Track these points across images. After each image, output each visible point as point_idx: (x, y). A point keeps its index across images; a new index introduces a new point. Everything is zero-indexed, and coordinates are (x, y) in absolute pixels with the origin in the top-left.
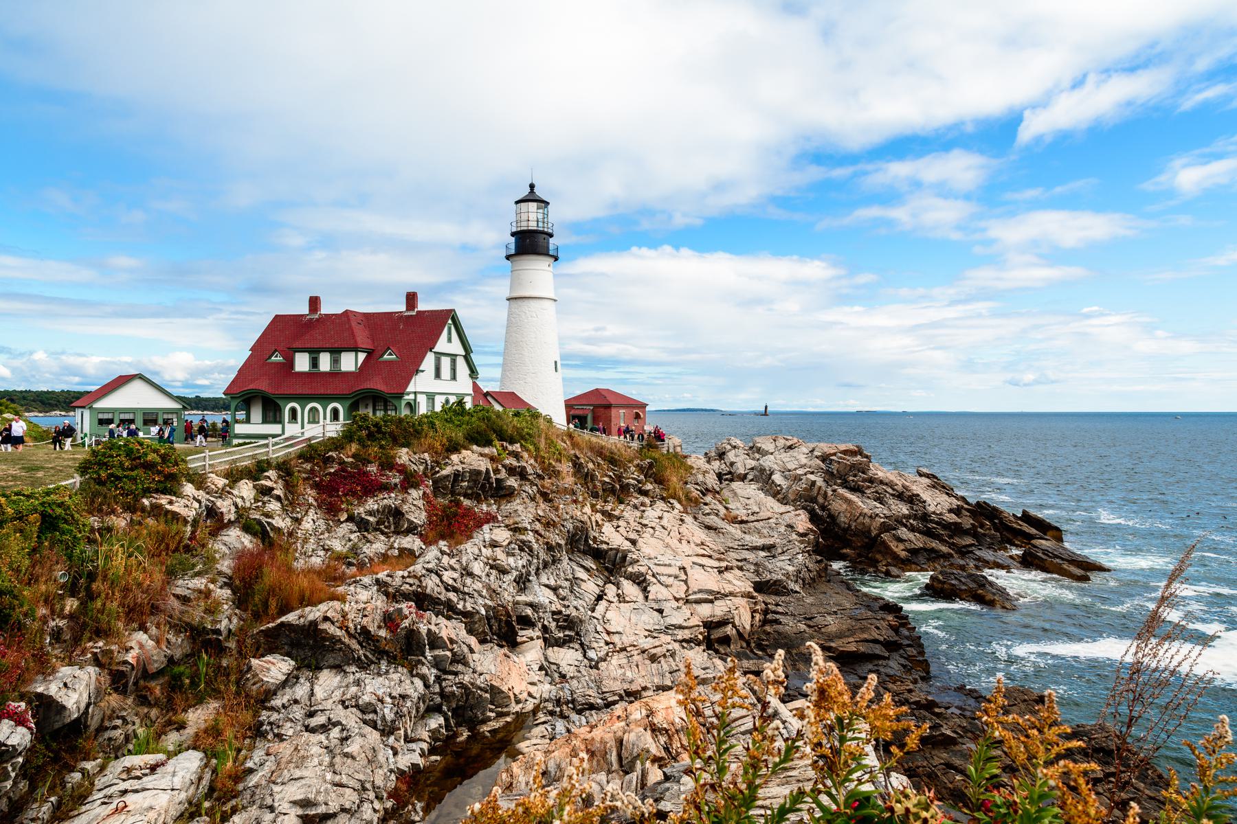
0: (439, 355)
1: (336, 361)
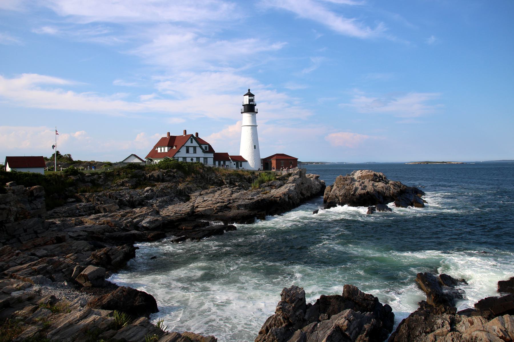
1: (164, 149)
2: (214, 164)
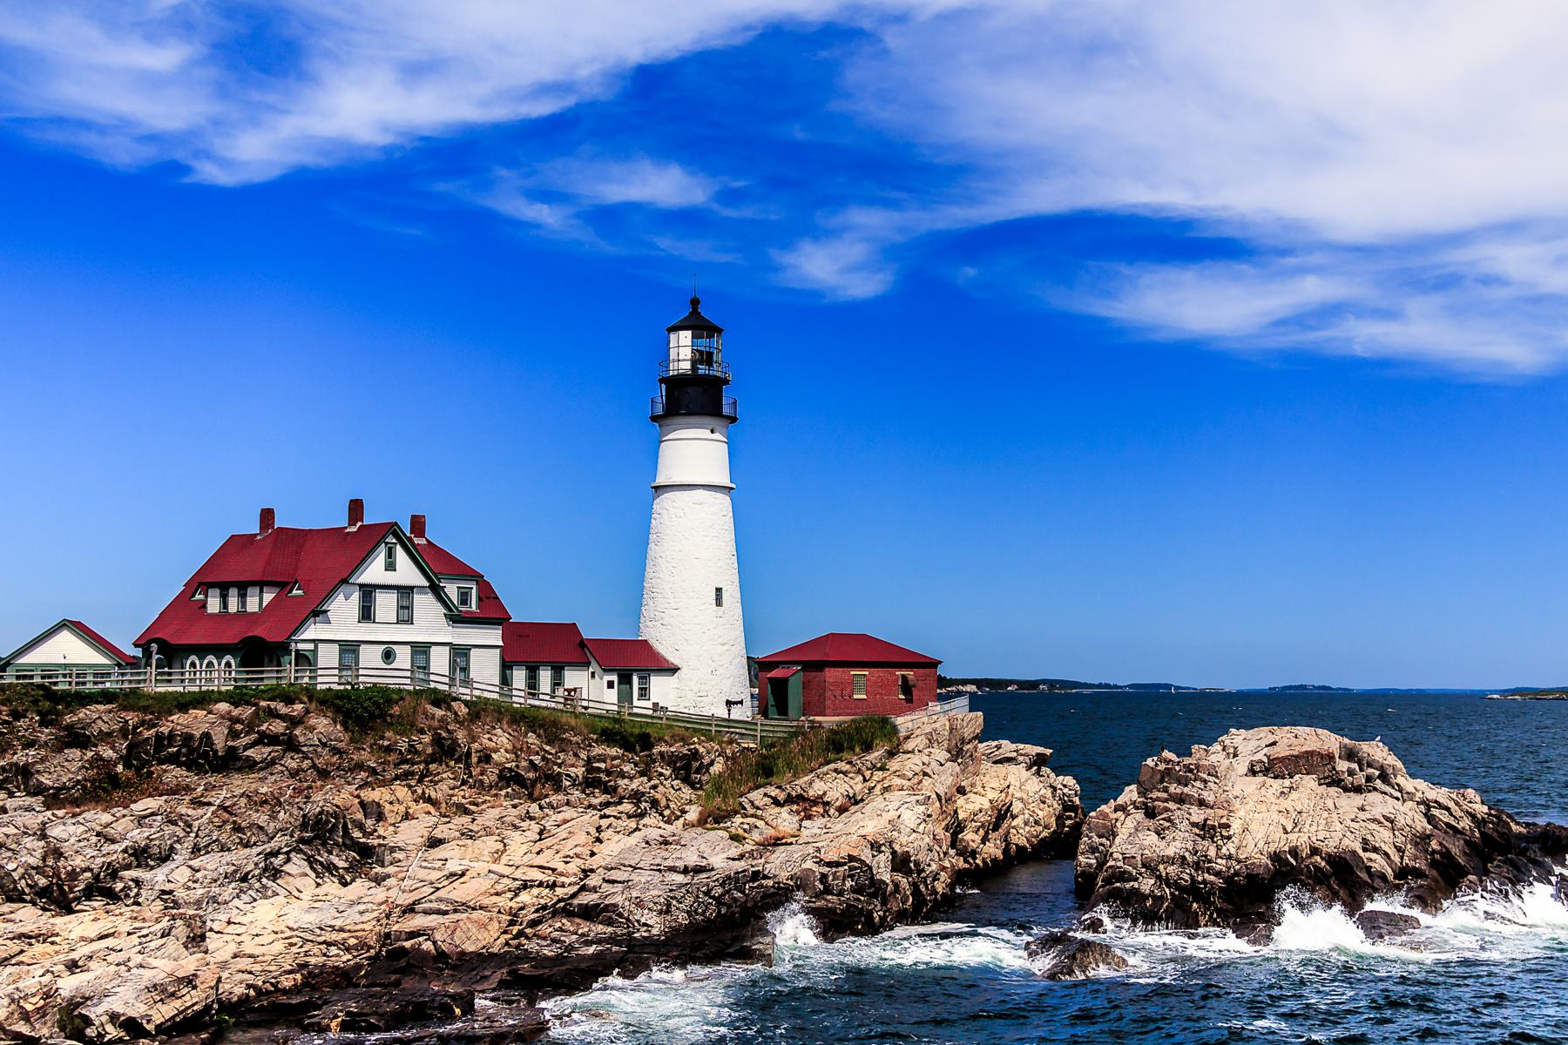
0: (368, 591)
2: (505, 681)
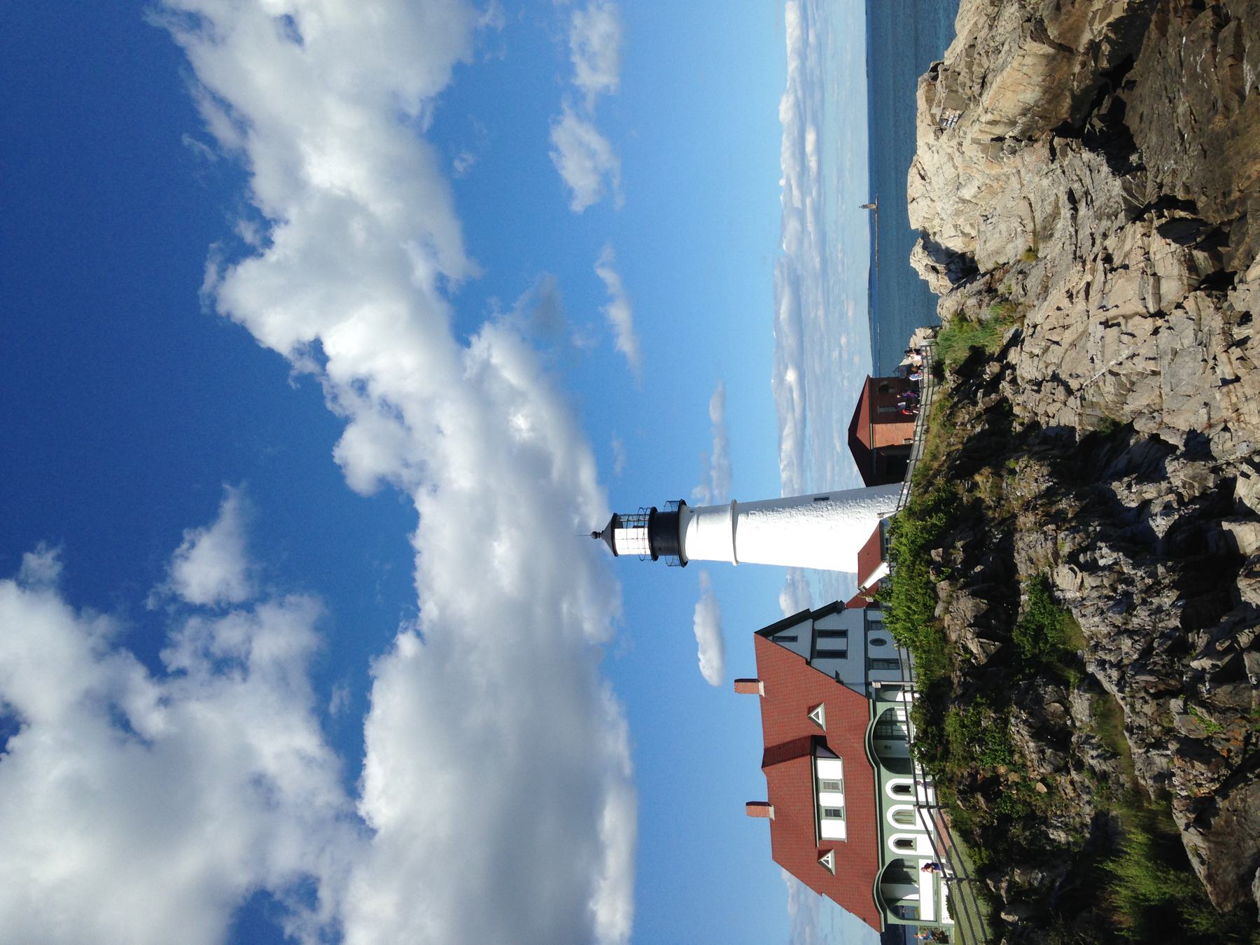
1: (832, 786)
